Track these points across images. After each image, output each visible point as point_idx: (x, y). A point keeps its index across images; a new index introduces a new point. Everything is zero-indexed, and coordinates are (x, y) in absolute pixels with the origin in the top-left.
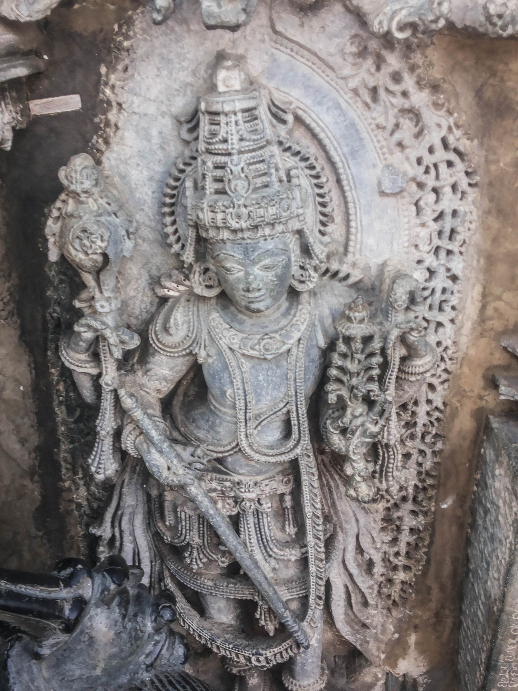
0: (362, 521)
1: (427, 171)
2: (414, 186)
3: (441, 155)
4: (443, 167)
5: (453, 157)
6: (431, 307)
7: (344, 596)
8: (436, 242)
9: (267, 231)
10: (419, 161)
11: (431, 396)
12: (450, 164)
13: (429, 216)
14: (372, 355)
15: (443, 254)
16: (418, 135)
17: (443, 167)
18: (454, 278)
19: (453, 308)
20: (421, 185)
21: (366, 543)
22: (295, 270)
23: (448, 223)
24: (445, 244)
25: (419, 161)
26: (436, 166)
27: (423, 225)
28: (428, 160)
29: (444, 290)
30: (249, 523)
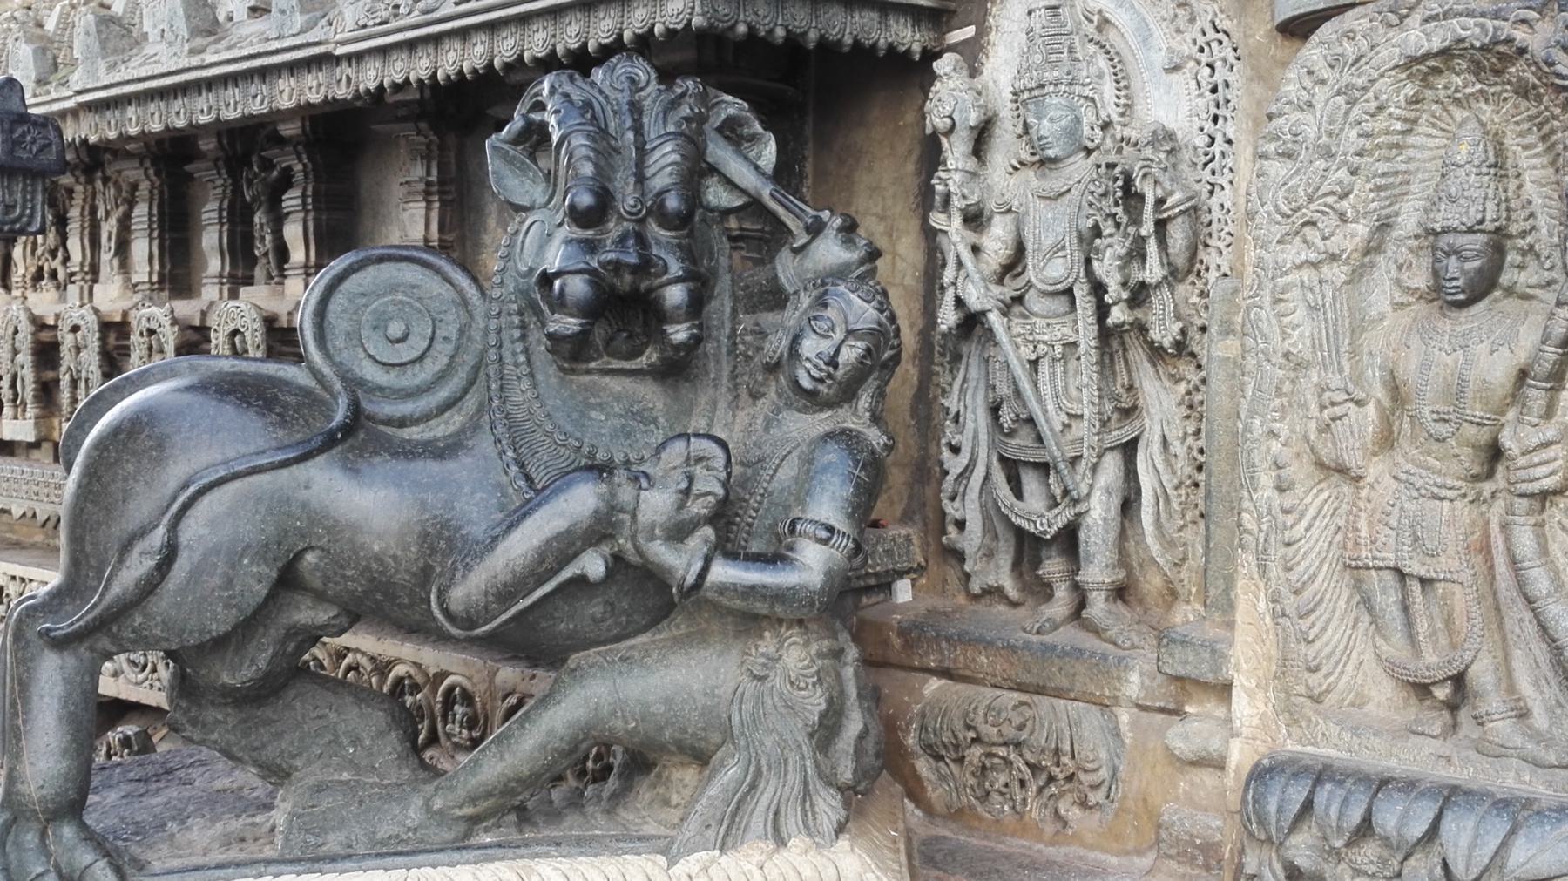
0: (1165, 404)
1: (1202, 50)
2: (1192, 64)
3: (1211, 34)
4: (1214, 45)
5: (1221, 36)
6: (1213, 173)
7: (1152, 501)
8: (1213, 110)
9: (1051, 88)
10: (1195, 42)
11: (1219, 261)
12: (1221, 43)
13: (1206, 87)
14: (1116, 179)
15: (1221, 121)
16: (1192, 20)
17: (1214, 45)
18: (1229, 142)
19: (1231, 170)
20: (1199, 63)
21: (1173, 434)
22: (1086, 131)
23: (1220, 95)
24: (1222, 112)
25: (1195, 42)
26: (1208, 44)
27: (1201, 95)
28: (1201, 41)
29: (1223, 154)
30: (1044, 366)
